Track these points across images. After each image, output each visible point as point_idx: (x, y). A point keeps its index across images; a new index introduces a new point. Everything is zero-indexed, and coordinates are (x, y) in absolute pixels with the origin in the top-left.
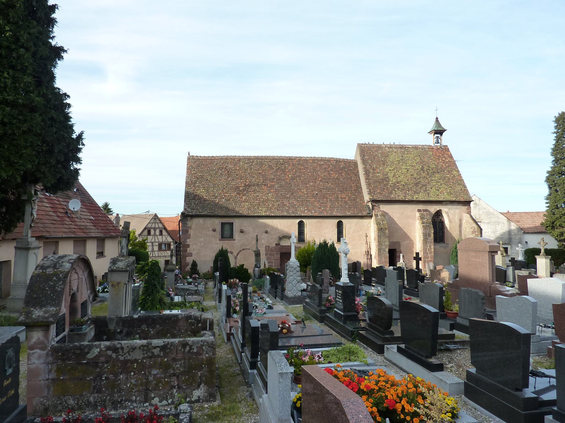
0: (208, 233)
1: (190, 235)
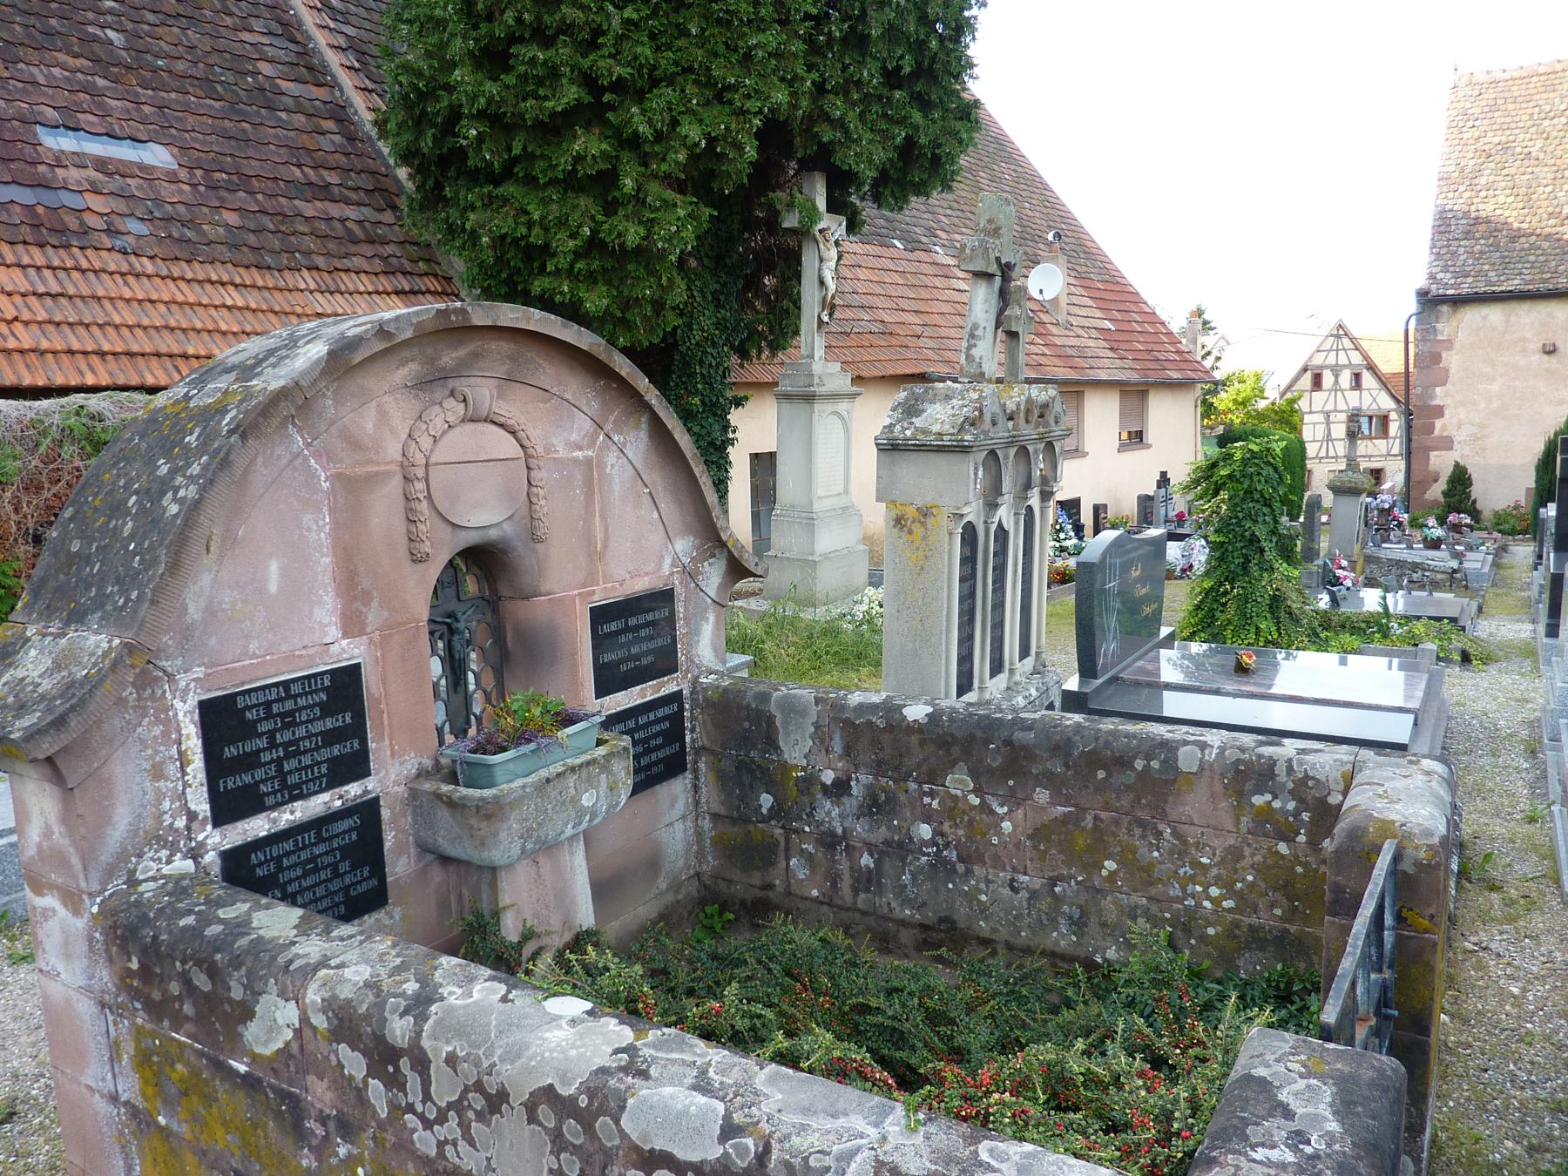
0: (1523, 362)
1: (1447, 371)
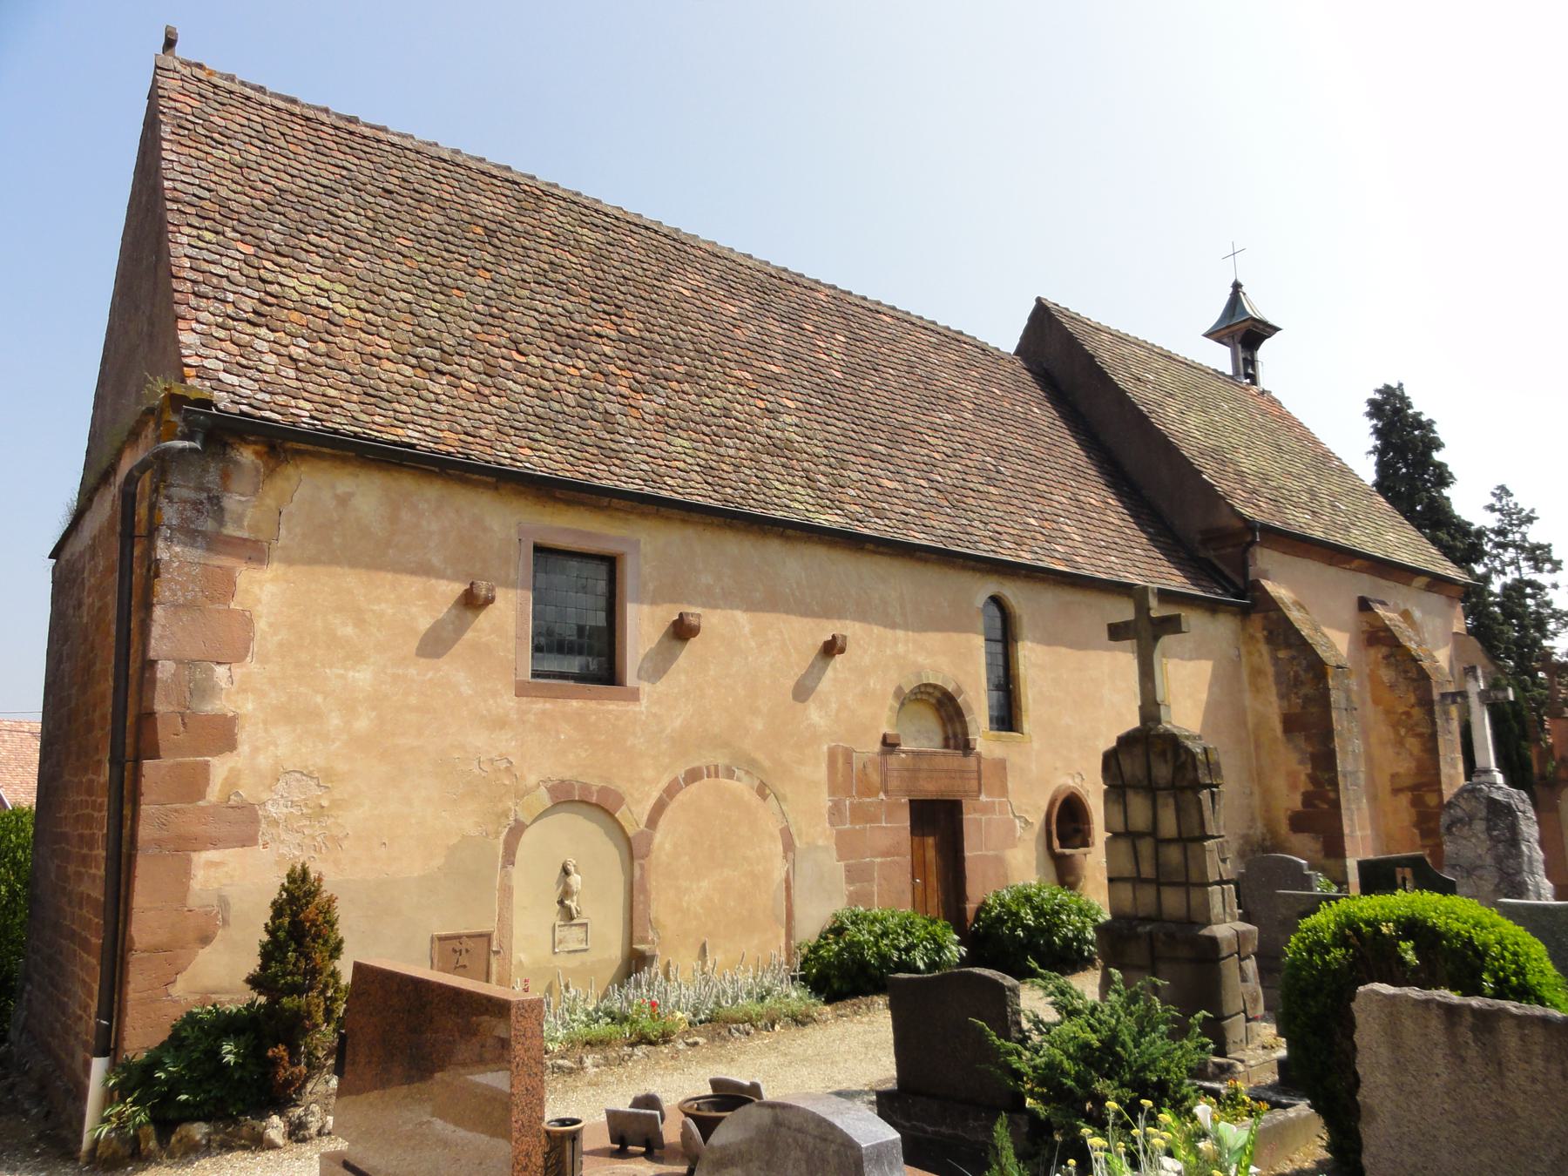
1: (247, 621)
